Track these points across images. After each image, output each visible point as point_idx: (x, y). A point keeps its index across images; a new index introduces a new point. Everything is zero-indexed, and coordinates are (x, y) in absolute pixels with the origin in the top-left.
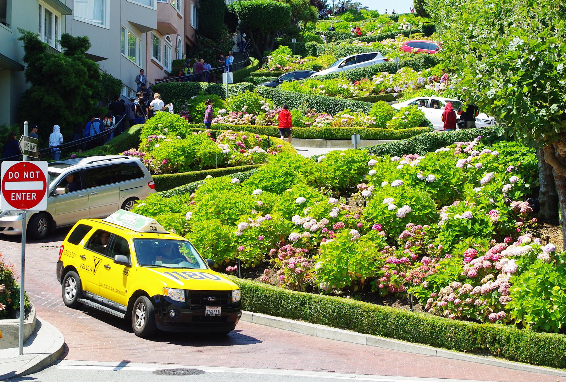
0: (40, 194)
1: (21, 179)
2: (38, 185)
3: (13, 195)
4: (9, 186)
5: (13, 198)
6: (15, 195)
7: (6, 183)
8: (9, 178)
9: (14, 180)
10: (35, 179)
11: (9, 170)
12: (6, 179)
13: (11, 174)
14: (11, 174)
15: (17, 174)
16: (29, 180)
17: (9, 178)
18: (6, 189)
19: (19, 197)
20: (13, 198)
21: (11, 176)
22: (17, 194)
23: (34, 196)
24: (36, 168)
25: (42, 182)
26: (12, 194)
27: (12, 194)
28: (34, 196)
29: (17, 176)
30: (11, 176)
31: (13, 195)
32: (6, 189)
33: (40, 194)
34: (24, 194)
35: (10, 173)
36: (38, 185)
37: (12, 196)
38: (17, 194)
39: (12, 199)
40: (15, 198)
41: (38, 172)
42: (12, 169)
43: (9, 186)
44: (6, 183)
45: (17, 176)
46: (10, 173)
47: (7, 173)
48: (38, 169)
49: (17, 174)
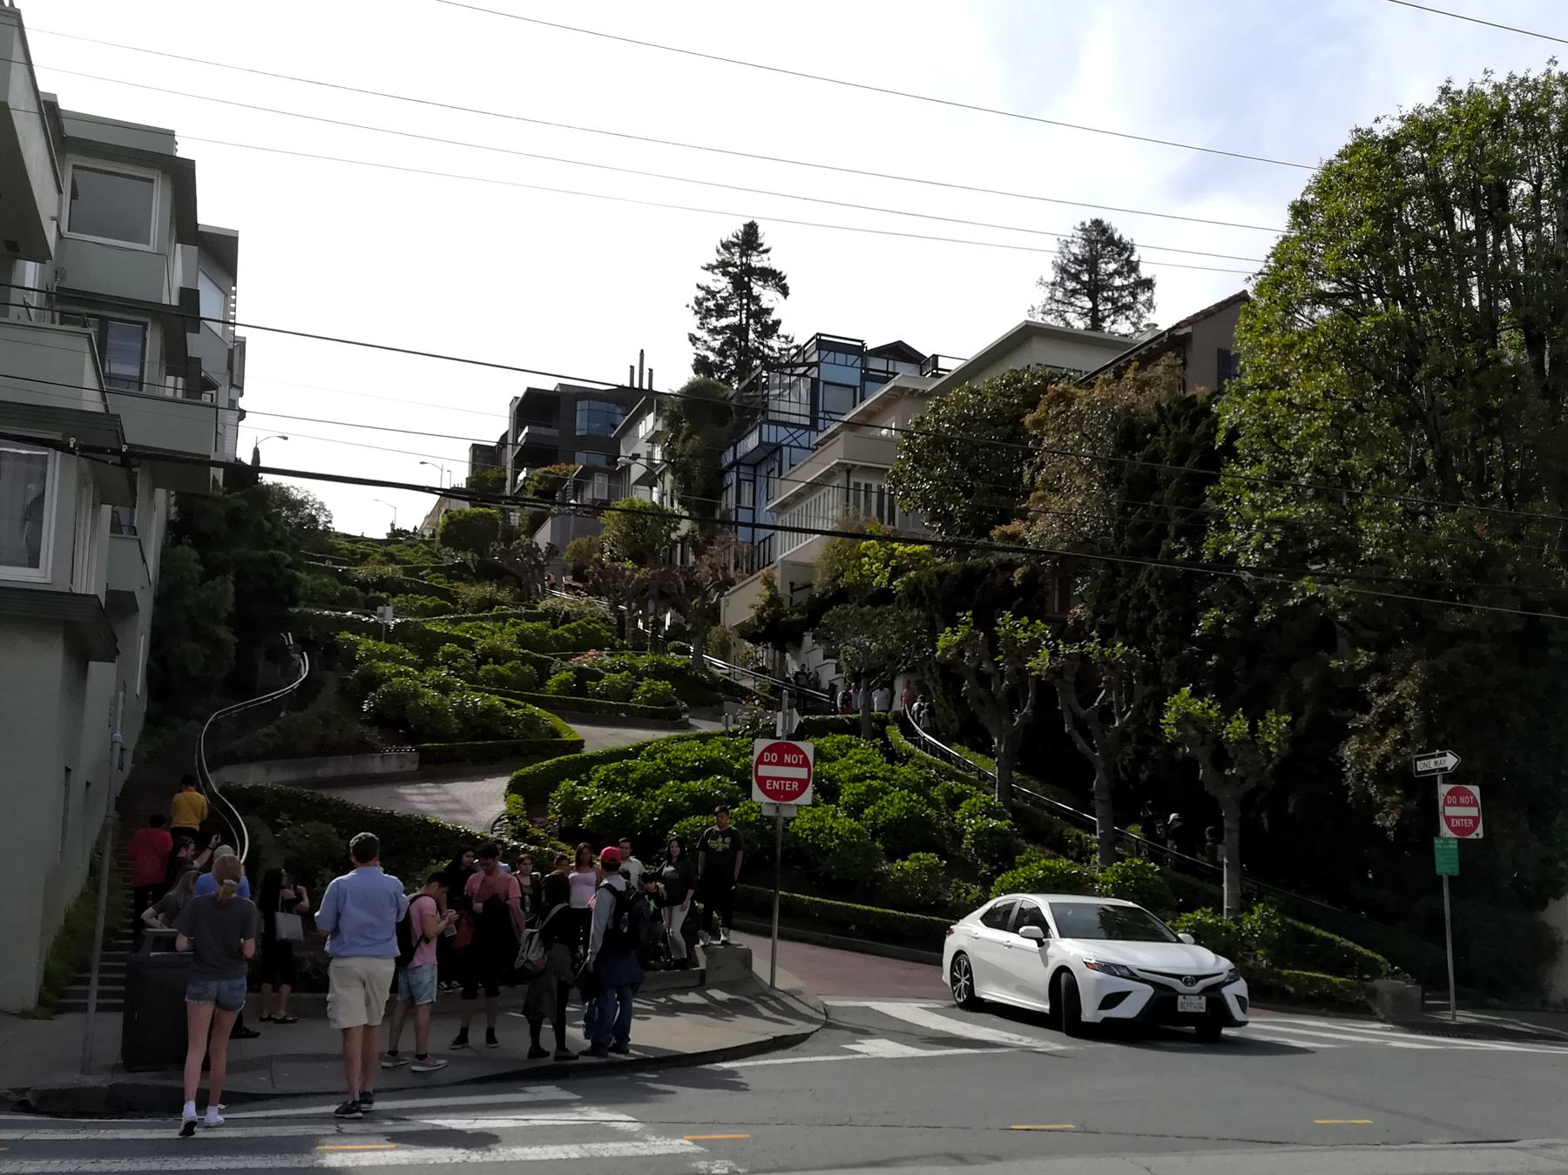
0: (803, 784)
1: (781, 763)
2: (802, 773)
4: (764, 771)
7: (760, 767)
9: (770, 763)
10: (797, 765)
11: (766, 750)
12: (760, 761)
16: (791, 765)
18: (760, 774)
19: (776, 785)
23: (795, 786)
24: (799, 751)
25: (805, 770)
28: (795, 786)
32: (760, 774)
33: (803, 784)
34: (783, 782)
36: (802, 773)
41: (801, 756)
42: (769, 749)
43: (764, 771)
44: (760, 767)
47: (762, 754)
48: (803, 753)
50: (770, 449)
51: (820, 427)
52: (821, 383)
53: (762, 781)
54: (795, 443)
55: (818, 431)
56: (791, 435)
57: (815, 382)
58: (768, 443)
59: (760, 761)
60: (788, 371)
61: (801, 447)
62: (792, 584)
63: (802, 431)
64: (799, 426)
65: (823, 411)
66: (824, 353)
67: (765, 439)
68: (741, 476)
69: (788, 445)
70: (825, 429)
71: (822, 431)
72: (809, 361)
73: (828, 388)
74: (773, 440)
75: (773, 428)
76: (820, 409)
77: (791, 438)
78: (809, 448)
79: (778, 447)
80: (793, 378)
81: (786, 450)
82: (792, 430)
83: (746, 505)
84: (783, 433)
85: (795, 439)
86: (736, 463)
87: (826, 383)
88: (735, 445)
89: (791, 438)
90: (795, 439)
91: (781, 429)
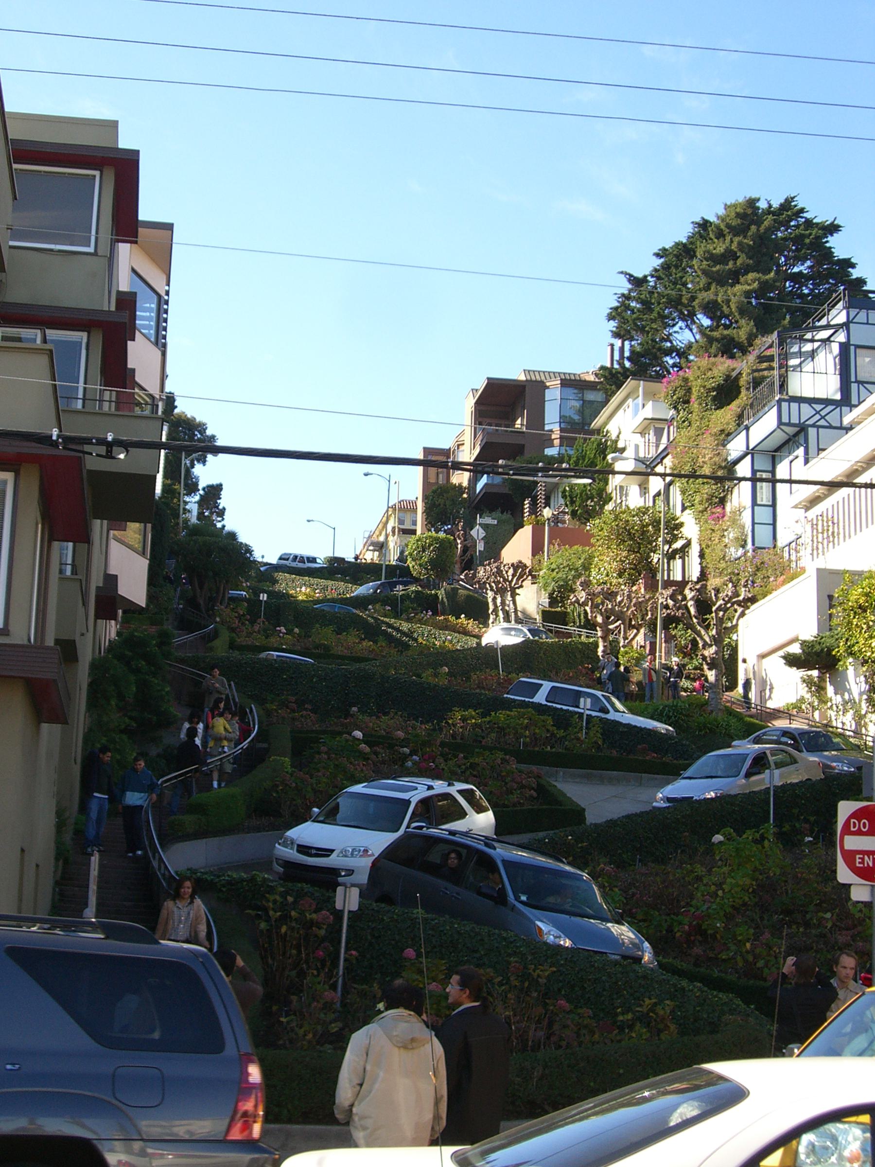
3: (859, 858)
4: (852, 843)
5: (860, 863)
6: (863, 859)
7: (846, 838)
8: (852, 829)
9: (859, 833)
11: (853, 816)
12: (847, 830)
13: (854, 823)
14: (854, 823)
15: (864, 823)
17: (852, 829)
18: (846, 848)
20: (860, 863)
21: (854, 827)
22: (866, 857)
26: (858, 856)
27: (858, 856)
29: (864, 827)
30: (854, 827)
31: (859, 858)
35: (852, 821)
37: (858, 860)
38: (866, 857)
39: (858, 865)
40: (863, 862)
42: (857, 815)
43: (852, 843)
44: (846, 838)
45: (864, 827)
46: (852, 821)
47: (847, 823)
49: (864, 823)
50: (791, 430)
51: (854, 401)
52: (852, 348)
53: (850, 856)
54: (822, 423)
55: (852, 407)
56: (818, 412)
57: (845, 348)
58: (789, 424)
59: (847, 830)
60: (809, 336)
61: (830, 427)
62: (830, 597)
63: (830, 408)
64: (826, 402)
65: (856, 381)
66: (853, 312)
67: (785, 419)
68: (756, 468)
69: (813, 426)
70: (860, 403)
71: (856, 406)
72: (832, 323)
73: (858, 350)
74: (795, 420)
75: (794, 406)
76: (853, 379)
77: (817, 417)
78: (841, 428)
79: (802, 429)
80: (816, 344)
81: (812, 432)
82: (818, 407)
83: (764, 502)
84: (807, 411)
85: (823, 417)
86: (750, 452)
87: (857, 347)
88: (747, 428)
89: (817, 417)
90: (823, 417)
91: (805, 407)
